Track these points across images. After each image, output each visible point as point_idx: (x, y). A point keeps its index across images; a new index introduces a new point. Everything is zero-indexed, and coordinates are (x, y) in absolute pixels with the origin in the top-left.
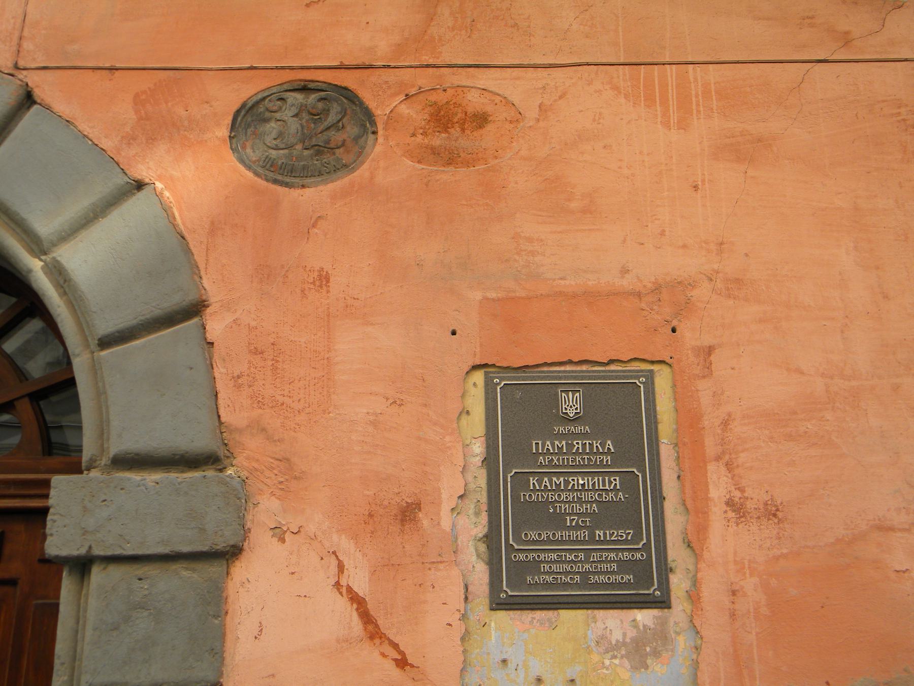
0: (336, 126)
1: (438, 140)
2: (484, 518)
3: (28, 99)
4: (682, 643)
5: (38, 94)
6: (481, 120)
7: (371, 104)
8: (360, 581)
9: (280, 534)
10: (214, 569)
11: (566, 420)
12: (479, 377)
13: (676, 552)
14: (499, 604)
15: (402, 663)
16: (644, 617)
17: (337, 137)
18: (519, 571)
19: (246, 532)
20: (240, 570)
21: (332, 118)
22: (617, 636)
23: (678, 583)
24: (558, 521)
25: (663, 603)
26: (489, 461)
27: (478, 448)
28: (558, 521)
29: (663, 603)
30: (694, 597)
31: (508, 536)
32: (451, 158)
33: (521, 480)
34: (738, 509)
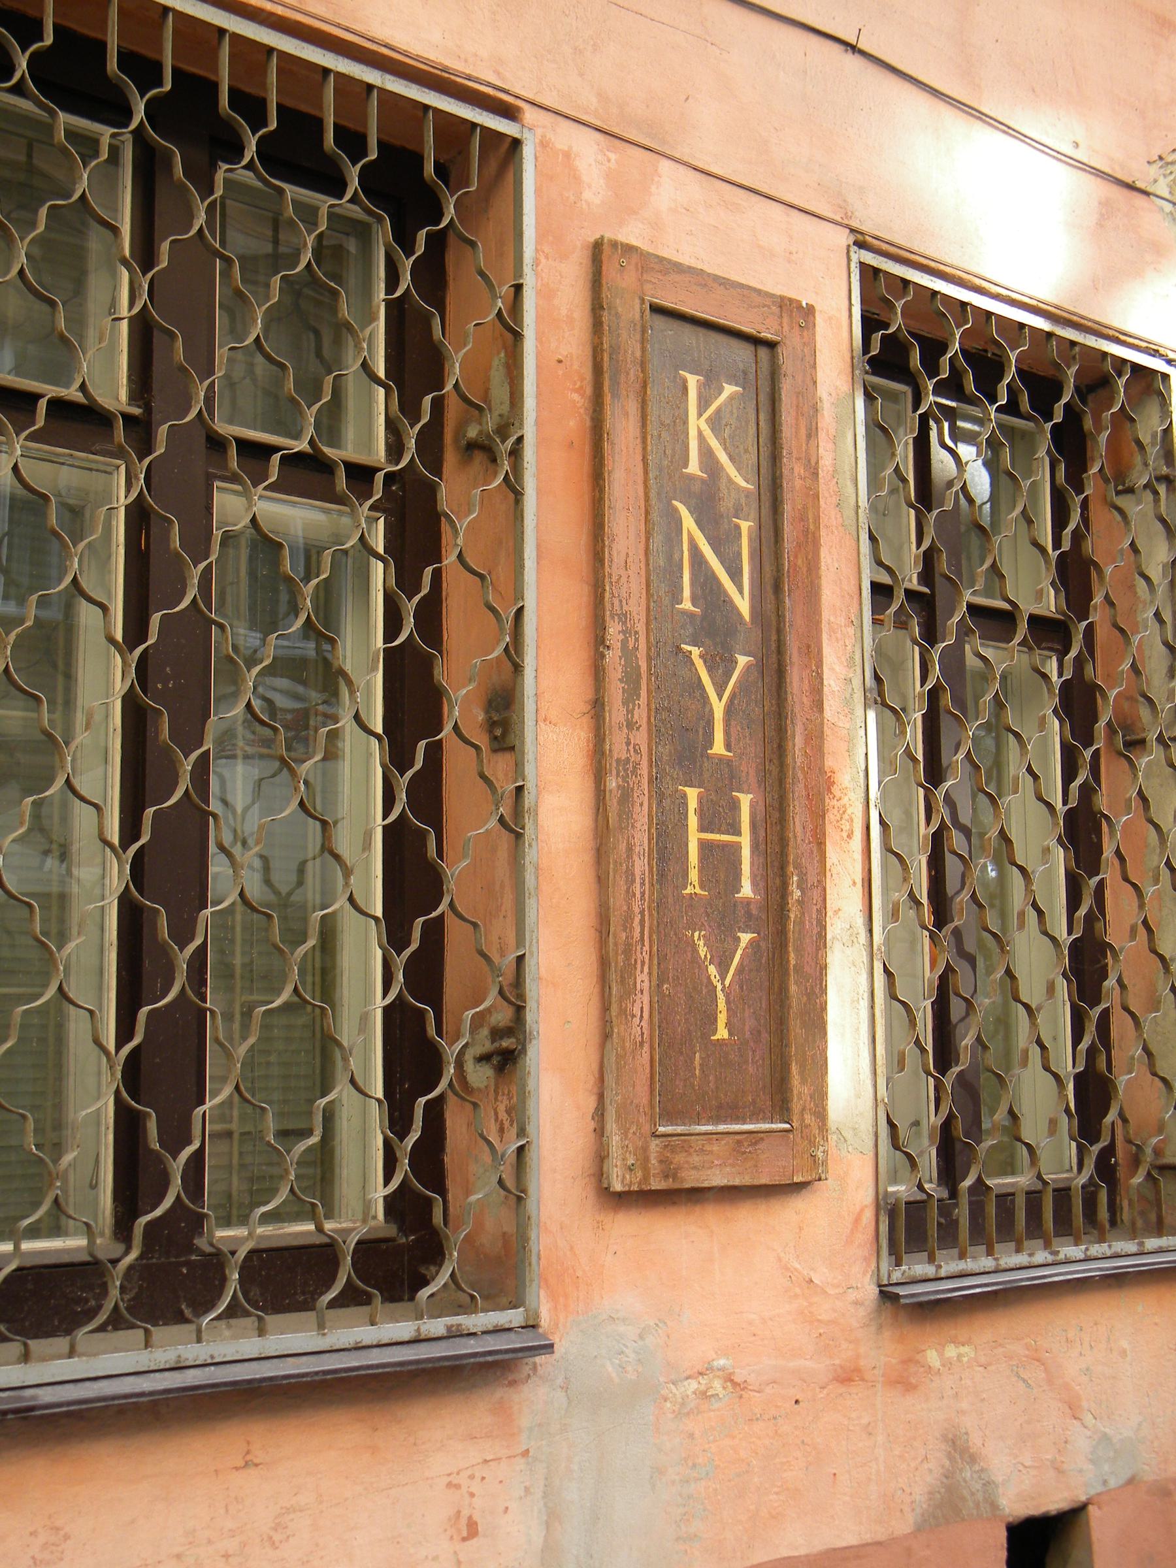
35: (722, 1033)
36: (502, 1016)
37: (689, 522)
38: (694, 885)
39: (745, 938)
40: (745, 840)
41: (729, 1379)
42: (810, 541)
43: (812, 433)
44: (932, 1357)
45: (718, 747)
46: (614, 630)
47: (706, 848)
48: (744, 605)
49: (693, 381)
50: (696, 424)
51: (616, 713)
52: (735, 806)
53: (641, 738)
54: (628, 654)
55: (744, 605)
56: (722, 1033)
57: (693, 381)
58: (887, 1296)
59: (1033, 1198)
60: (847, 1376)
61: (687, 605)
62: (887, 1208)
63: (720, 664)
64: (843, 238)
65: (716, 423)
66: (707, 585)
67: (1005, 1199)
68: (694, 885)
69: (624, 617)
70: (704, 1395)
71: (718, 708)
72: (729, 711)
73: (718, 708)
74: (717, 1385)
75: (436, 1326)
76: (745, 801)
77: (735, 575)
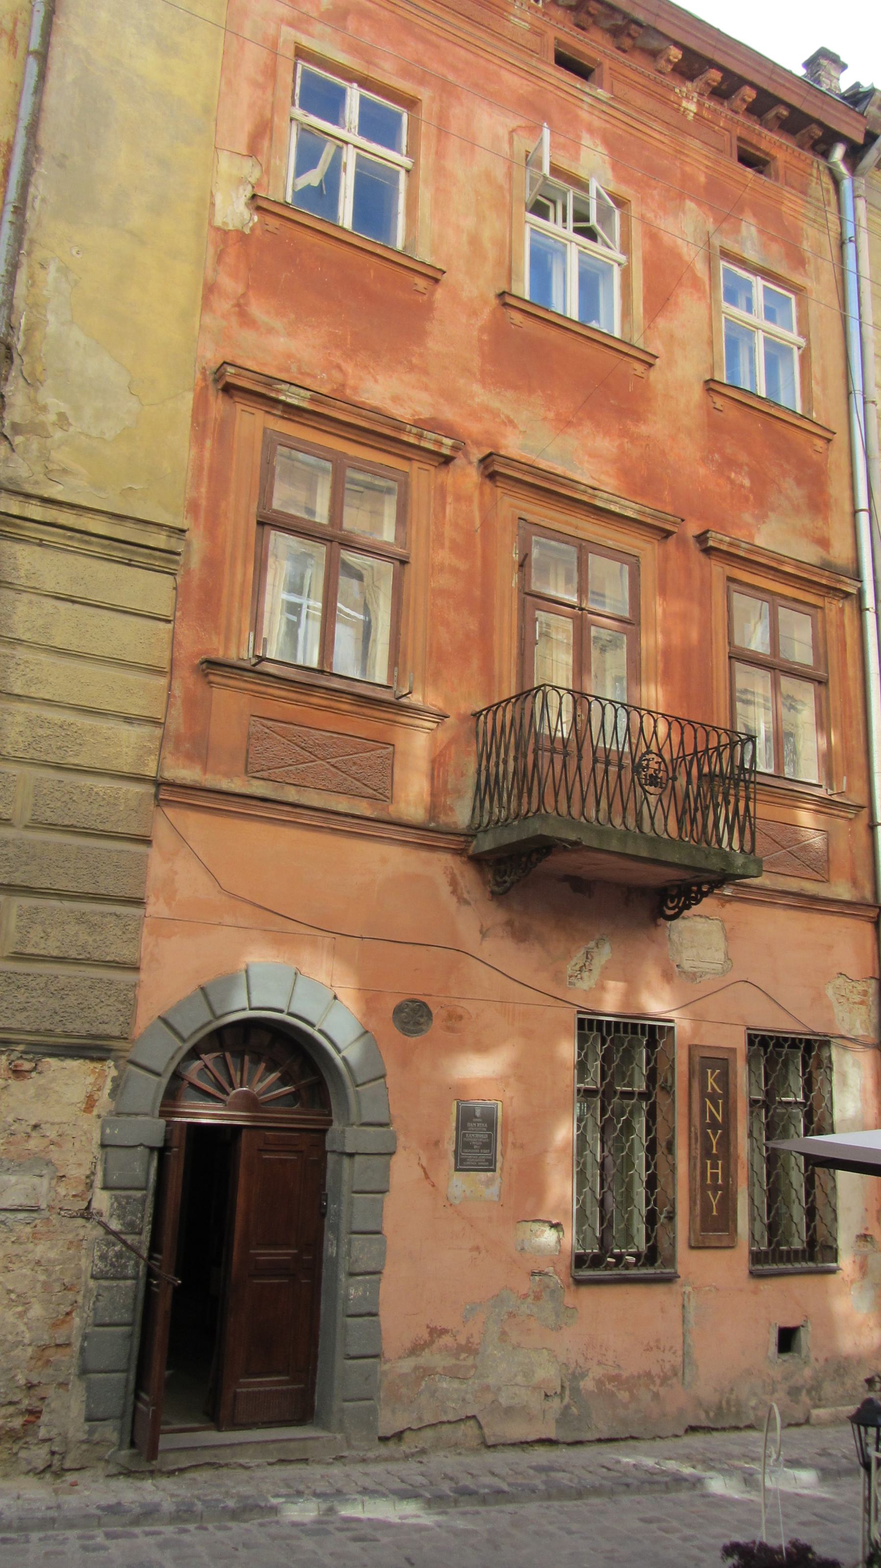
0: (422, 1016)
1: (449, 1024)
2: (454, 1146)
3: (335, 997)
4: (499, 1180)
5: (338, 996)
6: (461, 1017)
7: (431, 1009)
8: (424, 1162)
9: (405, 1148)
10: (387, 1157)
11: (476, 1117)
12: (455, 1102)
13: (499, 1157)
14: (457, 1170)
15: (433, 1186)
16: (489, 1174)
17: (422, 1020)
18: (463, 1161)
19: (396, 1147)
20: (394, 1158)
21: (419, 1014)
22: (483, 1179)
23: (498, 1165)
24: (472, 1147)
25: (494, 1170)
26: (457, 1129)
27: (454, 1124)
28: (472, 1147)
29: (494, 1170)
30: (502, 1169)
31: (460, 1150)
32: (450, 1029)
33: (464, 1135)
34: (514, 1144)
35: (715, 1213)
36: (671, 1209)
37: (708, 1103)
38: (709, 1182)
39: (720, 1192)
40: (720, 1171)
41: (715, 1287)
42: (735, 1102)
43: (736, 1078)
44: (762, 1288)
45: (714, 1151)
46: (693, 1129)
47: (711, 1173)
48: (720, 1119)
49: (709, 1071)
50: (710, 1080)
51: (693, 1146)
52: (718, 1164)
53: (698, 1152)
54: (696, 1134)
55: (720, 1119)
56: (715, 1213)
57: (709, 1071)
58: (751, 1273)
59: (788, 1252)
60: (741, 1290)
61: (708, 1121)
62: (751, 1253)
63: (715, 1134)
64: (744, 1028)
65: (714, 1080)
66: (712, 1115)
67: (782, 1252)
68: (709, 1182)
69: (695, 1126)
70: (710, 1290)
71: (714, 1143)
72: (717, 1143)
73: (714, 1143)
74: (713, 1289)
75: (658, 1271)
76: (720, 1162)
77: (718, 1113)
